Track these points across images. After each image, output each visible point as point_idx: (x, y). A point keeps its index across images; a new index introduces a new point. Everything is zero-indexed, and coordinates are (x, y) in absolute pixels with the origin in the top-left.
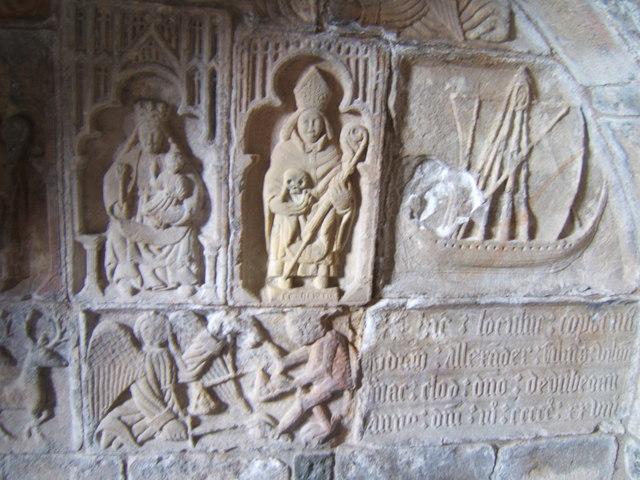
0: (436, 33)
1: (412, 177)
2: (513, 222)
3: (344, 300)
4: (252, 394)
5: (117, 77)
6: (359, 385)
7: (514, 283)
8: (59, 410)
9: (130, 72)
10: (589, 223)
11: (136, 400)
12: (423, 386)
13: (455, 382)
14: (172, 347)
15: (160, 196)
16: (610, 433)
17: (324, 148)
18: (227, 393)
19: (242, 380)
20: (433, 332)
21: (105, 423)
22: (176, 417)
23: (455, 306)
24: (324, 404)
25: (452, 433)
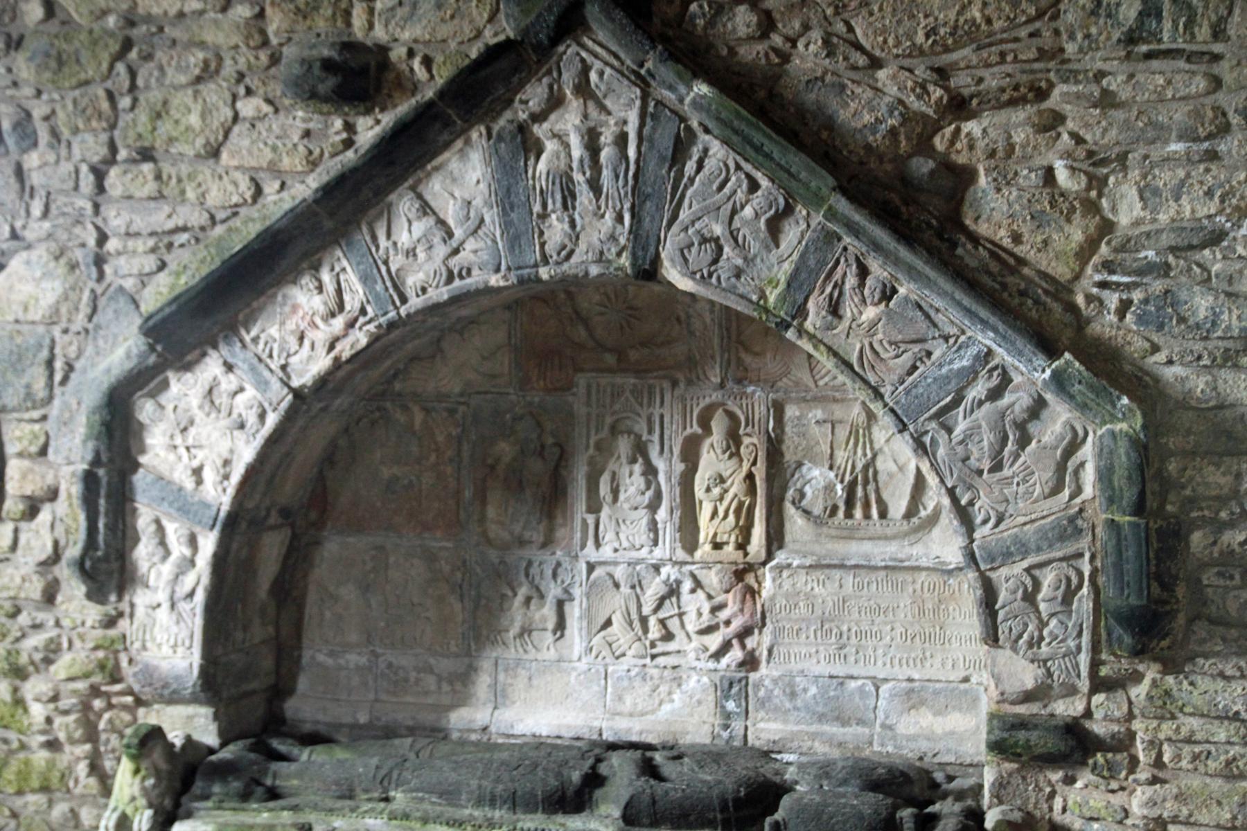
0: (797, 384)
1: (793, 475)
2: (867, 506)
3: (748, 559)
4: (691, 628)
5: (609, 420)
6: (764, 625)
7: (876, 551)
8: (567, 632)
9: (615, 417)
11: (616, 627)
12: (813, 628)
13: (838, 627)
14: (638, 589)
15: (632, 490)
16: (979, 684)
17: (730, 457)
18: (674, 625)
19: (684, 618)
20: (824, 590)
21: (597, 640)
22: (640, 639)
23: (829, 566)
25: (839, 669)
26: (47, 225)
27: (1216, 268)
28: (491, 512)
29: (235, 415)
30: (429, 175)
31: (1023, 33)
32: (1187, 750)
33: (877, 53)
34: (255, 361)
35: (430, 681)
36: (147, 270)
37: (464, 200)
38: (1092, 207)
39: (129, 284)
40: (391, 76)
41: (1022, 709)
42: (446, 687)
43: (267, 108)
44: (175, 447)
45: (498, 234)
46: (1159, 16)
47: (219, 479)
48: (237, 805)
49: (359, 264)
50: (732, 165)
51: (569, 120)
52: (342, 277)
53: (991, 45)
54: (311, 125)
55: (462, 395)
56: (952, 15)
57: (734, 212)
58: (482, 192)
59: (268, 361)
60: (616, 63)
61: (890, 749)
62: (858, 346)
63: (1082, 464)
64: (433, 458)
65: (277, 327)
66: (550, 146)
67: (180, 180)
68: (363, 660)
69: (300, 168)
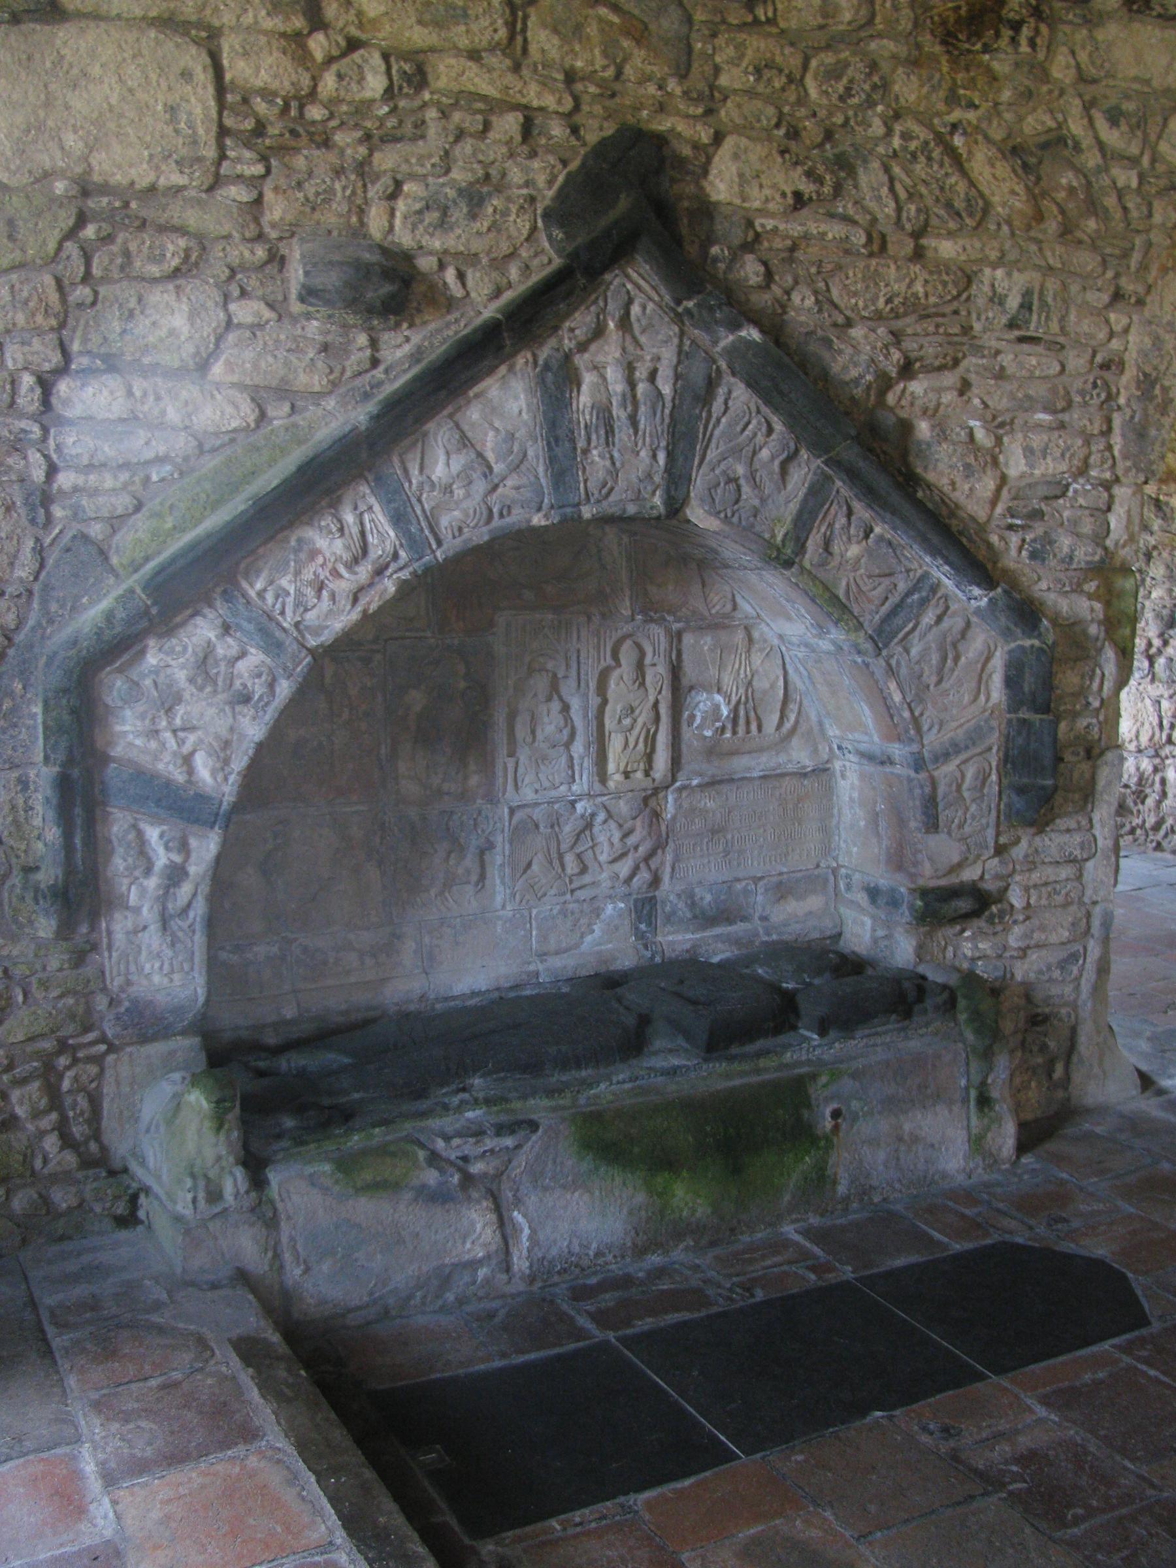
0: (694, 612)
2: (748, 723)
4: (603, 858)
5: (527, 659)
7: (753, 763)
8: (487, 882)
10: (792, 717)
11: (535, 867)
21: (519, 885)
24: (647, 859)
27: (1066, 514)
28: (402, 767)
29: (237, 684)
30: (469, 402)
31: (948, 309)
32: (1043, 890)
33: (848, 313)
34: (264, 619)
36: (120, 511)
37: (507, 432)
38: (995, 462)
39: (96, 530)
40: (419, 288)
41: (943, 882)
42: (369, 961)
43: (267, 314)
44: (157, 732)
45: (541, 469)
46: (1030, 309)
47: (218, 765)
49: (389, 502)
50: (753, 409)
51: (610, 351)
52: (366, 517)
53: (928, 316)
54: (329, 338)
55: (376, 640)
56: (903, 286)
57: (754, 453)
58: (526, 424)
59: (280, 618)
60: (656, 298)
61: (775, 937)
62: (844, 583)
63: (990, 676)
64: (346, 715)
65: (289, 577)
66: (588, 378)
67: (158, 398)
68: (275, 949)
69: (317, 388)
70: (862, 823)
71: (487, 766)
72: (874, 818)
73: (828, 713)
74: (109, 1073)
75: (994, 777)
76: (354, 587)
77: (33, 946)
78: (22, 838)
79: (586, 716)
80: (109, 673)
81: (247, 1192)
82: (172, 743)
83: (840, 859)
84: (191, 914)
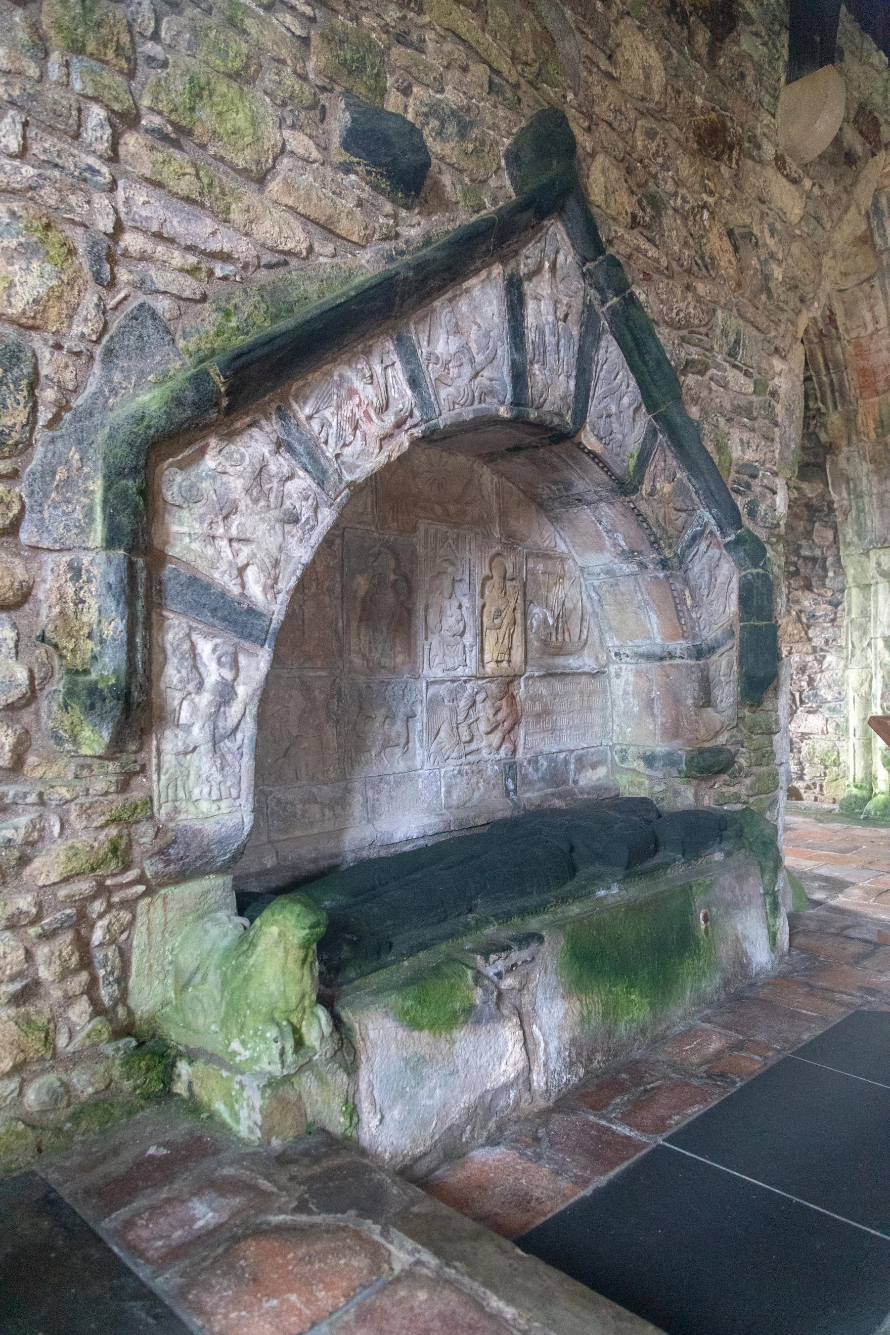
8: (410, 745)
11: (442, 734)
26: (28, 171)
29: (288, 503)
35: (315, 809)
39: (163, 305)
42: (328, 813)
43: (315, 154)
47: (269, 582)
48: (374, 964)
69: (355, 238)
70: (636, 709)
71: (410, 648)
72: (649, 704)
73: (611, 628)
74: (141, 920)
75: (735, 668)
76: (381, 433)
77: (72, 767)
78: (70, 635)
79: (474, 613)
80: (171, 465)
81: (331, 1035)
82: (227, 553)
83: (614, 738)
84: (239, 736)
